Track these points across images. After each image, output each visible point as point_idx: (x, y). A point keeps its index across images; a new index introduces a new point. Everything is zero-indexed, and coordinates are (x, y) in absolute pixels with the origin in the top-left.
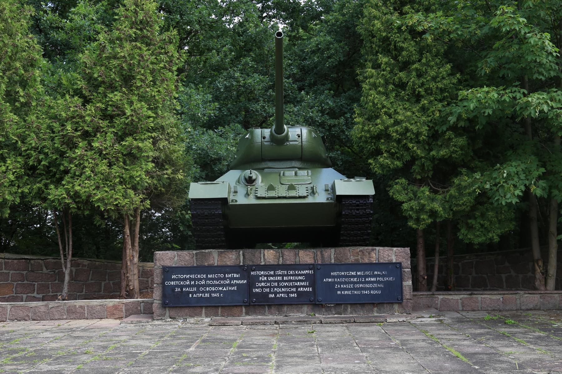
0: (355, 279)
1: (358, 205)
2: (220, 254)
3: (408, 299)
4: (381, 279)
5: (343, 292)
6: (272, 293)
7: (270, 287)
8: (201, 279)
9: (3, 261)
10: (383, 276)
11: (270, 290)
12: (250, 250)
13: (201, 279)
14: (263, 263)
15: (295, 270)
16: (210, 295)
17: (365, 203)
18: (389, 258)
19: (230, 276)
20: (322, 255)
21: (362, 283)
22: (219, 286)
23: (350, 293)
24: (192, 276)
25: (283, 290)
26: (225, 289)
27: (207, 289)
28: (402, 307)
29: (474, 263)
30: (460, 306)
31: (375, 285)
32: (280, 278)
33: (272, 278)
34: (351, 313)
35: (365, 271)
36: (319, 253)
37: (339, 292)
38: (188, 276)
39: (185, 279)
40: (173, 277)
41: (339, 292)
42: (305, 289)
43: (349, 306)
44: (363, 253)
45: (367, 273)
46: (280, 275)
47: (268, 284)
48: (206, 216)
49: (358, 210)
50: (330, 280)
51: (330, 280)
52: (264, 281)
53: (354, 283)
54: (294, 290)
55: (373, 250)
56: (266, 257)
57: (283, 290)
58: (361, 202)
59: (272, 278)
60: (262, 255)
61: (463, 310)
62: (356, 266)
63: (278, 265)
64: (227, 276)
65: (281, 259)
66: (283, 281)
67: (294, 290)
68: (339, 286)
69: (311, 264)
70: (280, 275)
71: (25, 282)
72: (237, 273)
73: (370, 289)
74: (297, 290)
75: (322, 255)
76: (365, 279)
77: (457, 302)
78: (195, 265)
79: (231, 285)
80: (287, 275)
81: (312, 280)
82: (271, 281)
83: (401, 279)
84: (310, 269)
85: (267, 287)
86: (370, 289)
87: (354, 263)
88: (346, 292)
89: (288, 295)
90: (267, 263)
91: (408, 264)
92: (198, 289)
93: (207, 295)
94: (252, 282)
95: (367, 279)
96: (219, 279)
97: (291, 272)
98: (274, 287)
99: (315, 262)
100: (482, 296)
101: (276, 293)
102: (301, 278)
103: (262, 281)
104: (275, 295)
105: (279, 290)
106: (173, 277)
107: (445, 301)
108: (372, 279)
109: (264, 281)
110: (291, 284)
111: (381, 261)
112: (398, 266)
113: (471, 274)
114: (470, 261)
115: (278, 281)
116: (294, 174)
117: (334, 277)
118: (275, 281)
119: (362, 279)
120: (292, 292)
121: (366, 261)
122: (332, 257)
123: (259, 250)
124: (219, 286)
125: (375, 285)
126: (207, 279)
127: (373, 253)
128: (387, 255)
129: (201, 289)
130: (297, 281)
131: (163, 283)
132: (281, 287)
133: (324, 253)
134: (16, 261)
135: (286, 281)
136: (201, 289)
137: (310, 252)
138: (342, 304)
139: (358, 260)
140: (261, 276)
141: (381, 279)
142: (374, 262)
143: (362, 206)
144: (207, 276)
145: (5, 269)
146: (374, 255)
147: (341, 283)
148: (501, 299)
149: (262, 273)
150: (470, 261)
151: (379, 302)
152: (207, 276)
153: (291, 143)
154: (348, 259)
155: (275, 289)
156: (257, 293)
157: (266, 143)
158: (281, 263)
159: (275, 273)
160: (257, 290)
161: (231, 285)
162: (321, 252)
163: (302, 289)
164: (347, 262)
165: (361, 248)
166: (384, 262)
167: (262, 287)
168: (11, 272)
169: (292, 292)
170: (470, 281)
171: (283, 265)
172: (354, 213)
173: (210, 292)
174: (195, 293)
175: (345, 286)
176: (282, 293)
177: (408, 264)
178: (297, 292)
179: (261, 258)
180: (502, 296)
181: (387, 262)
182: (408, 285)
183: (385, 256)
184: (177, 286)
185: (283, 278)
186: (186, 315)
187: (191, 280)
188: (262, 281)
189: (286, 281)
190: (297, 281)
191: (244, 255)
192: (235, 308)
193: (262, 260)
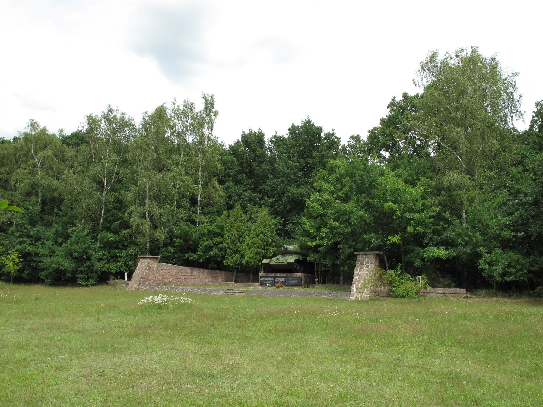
62: (294, 277)
81: (285, 280)
83: (302, 280)
94: (275, 280)
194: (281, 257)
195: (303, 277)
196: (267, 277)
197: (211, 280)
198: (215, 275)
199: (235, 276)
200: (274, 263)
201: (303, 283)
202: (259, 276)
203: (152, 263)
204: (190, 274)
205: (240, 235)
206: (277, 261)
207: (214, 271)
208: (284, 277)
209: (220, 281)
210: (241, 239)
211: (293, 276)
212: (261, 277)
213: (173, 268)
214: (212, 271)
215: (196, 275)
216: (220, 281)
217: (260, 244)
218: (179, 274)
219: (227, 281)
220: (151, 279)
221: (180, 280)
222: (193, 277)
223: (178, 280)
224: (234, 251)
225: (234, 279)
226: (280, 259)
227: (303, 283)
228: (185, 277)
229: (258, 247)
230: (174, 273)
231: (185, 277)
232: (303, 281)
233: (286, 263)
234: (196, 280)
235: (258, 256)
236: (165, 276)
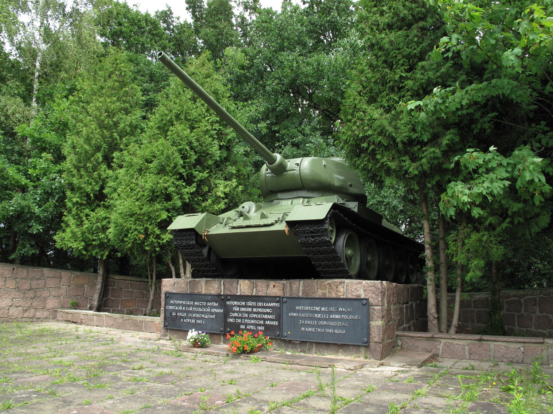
0: (319, 316)
1: (312, 232)
2: (207, 282)
3: (376, 342)
4: (345, 317)
5: (307, 329)
6: (243, 324)
7: (241, 318)
8: (189, 306)
9: (130, 282)
10: (349, 313)
11: (242, 321)
12: (229, 279)
13: (189, 306)
14: (238, 294)
15: (263, 301)
16: (196, 321)
17: (318, 230)
18: (357, 293)
19: (210, 304)
20: (291, 287)
21: (326, 320)
22: (202, 313)
23: (313, 330)
24: (184, 302)
25: (253, 321)
26: (206, 317)
27: (194, 315)
28: (370, 351)
29: (538, 299)
30: (467, 354)
31: (340, 323)
32: (250, 310)
33: (243, 309)
34: (316, 353)
35: (329, 306)
36: (288, 285)
37: (303, 329)
38: (181, 302)
39: (178, 305)
40: (172, 302)
41: (303, 329)
42: (272, 323)
43: (314, 345)
44: (331, 286)
45: (332, 309)
46: (250, 307)
47: (240, 315)
48: (184, 246)
49: (313, 237)
50: (295, 315)
51: (295, 315)
52: (237, 312)
53: (319, 319)
54: (262, 322)
55: (341, 283)
56: (242, 288)
57: (253, 321)
58: (315, 228)
59: (243, 309)
60: (239, 285)
61: (470, 359)
62: (324, 300)
63: (252, 296)
64: (208, 304)
65: (255, 290)
66: (253, 312)
67: (262, 322)
68: (303, 322)
69: (279, 297)
70: (250, 307)
71: (145, 299)
72: (216, 302)
73: (334, 327)
74: (264, 322)
75: (291, 287)
76: (329, 316)
77: (464, 349)
78: (188, 292)
79: (212, 313)
80: (257, 307)
82: (243, 312)
83: (369, 318)
84: (277, 302)
85: (239, 318)
86: (334, 327)
87: (321, 297)
88: (310, 329)
89: (256, 328)
90: (243, 294)
91: (379, 301)
92: (187, 315)
93: (193, 321)
94: (227, 311)
95: (331, 316)
96: (202, 307)
97: (260, 304)
98: (245, 318)
99: (284, 294)
100: (495, 343)
101: (246, 325)
102: (268, 310)
103: (235, 312)
104: (246, 327)
105: (249, 321)
106: (172, 302)
107: (448, 347)
108: (337, 317)
109: (237, 312)
110: (259, 316)
111: (349, 296)
112: (365, 303)
113: (534, 313)
114: (533, 297)
115: (248, 313)
116: (290, 203)
117: (298, 311)
118: (246, 312)
119: (326, 316)
120: (260, 325)
121: (334, 296)
122: (301, 290)
123: (237, 280)
124: (202, 313)
125: (340, 323)
126: (194, 306)
127: (340, 287)
128: (355, 289)
129: (190, 315)
130: (264, 313)
131: (165, 307)
132: (251, 319)
133: (293, 284)
134: (138, 283)
135: (255, 313)
136: (190, 315)
137: (279, 283)
138: (306, 342)
139: (325, 294)
140: (235, 306)
141: (345, 317)
142: (342, 297)
143: (315, 233)
144: (194, 303)
145: (131, 288)
146: (342, 289)
147: (305, 318)
148: (522, 349)
149: (236, 303)
150: (533, 297)
151: (343, 343)
152: (194, 303)
153: (289, 172)
154: (315, 292)
155: (246, 320)
156: (230, 322)
157: (267, 175)
158: (254, 294)
159: (246, 304)
160: (231, 320)
161: (212, 313)
162: (290, 284)
163: (269, 322)
164: (314, 296)
165: (330, 281)
166: (352, 297)
167: (235, 318)
168: (135, 291)
169: (260, 325)
170: (534, 320)
171: (255, 296)
172: (310, 242)
173: (196, 318)
174: (186, 318)
175: (309, 322)
176: (252, 324)
177: (379, 301)
178: (264, 325)
179: (237, 288)
180: (522, 345)
181: (355, 297)
182: (377, 326)
183: (353, 290)
184: (174, 310)
185: (252, 309)
186: (181, 338)
187: (183, 305)
188: (235, 312)
189: (255, 313)
190: (264, 313)
191: (224, 285)
192: (215, 336)
193: (238, 291)
194: (258, 208)
195: (375, 299)
196: (193, 296)
197: (19, 301)
198: (34, 283)
199: (99, 286)
200: (226, 230)
201: (376, 335)
202: (164, 289)
205: (114, 139)
206: (241, 222)
207: (35, 272)
208: (273, 299)
209: (51, 303)
210: (116, 154)
211: (319, 293)
212: (169, 295)
214: (23, 272)
216: (51, 303)
217: (168, 157)
219: (76, 306)
224: (88, 195)
225: (96, 297)
226: (252, 214)
227: (376, 335)
229: (162, 171)
232: (377, 323)
233: (282, 227)
235: (158, 206)
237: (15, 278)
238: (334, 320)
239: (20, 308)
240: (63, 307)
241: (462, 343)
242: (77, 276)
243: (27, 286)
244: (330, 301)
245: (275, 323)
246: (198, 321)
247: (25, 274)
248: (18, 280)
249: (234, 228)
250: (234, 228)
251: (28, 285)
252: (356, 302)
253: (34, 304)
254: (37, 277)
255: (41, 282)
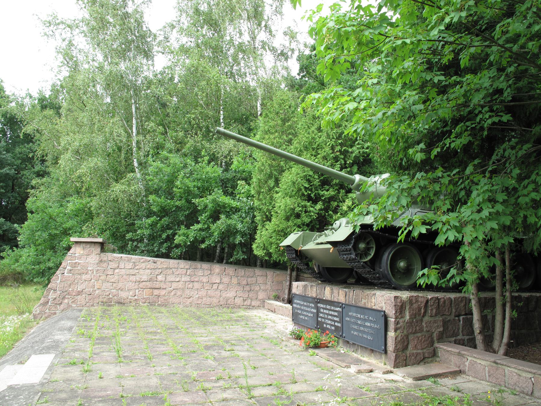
10: (374, 322)
35: (364, 314)
100: (509, 368)
101: (327, 324)
121: (369, 306)
197: (240, 293)
198: (249, 279)
203: (83, 255)
204: (187, 278)
207: (249, 271)
209: (261, 295)
213: (143, 265)
214: (242, 271)
215: (205, 280)
218: (160, 278)
220: (79, 293)
221: (163, 292)
222: (197, 285)
223: (156, 292)
228: (174, 285)
230: (145, 278)
231: (174, 285)
234: (203, 293)
236: (120, 285)
237: (237, 277)
238: (367, 327)
239: (242, 299)
240: (269, 299)
241: (483, 363)
242: (278, 275)
243: (245, 282)
244: (366, 311)
245: (339, 325)
246: (306, 318)
247: (243, 273)
248: (239, 278)
249: (318, 244)
250: (318, 244)
251: (245, 281)
252: (378, 313)
253: (250, 296)
254: (251, 275)
255: (254, 279)
